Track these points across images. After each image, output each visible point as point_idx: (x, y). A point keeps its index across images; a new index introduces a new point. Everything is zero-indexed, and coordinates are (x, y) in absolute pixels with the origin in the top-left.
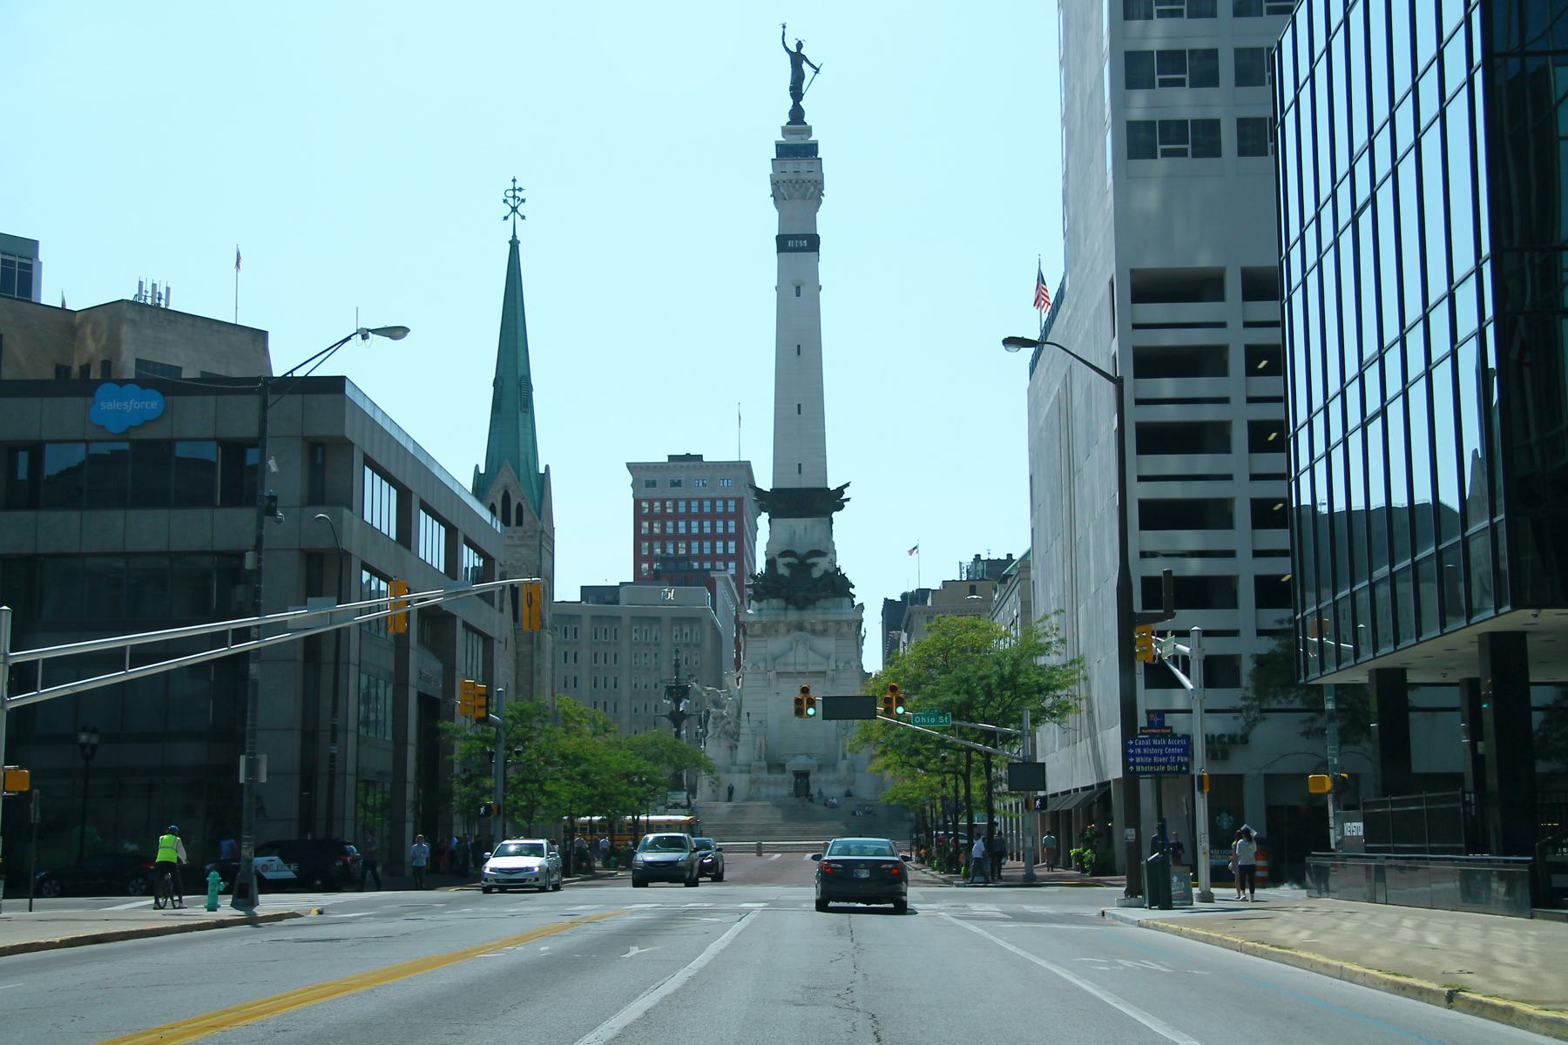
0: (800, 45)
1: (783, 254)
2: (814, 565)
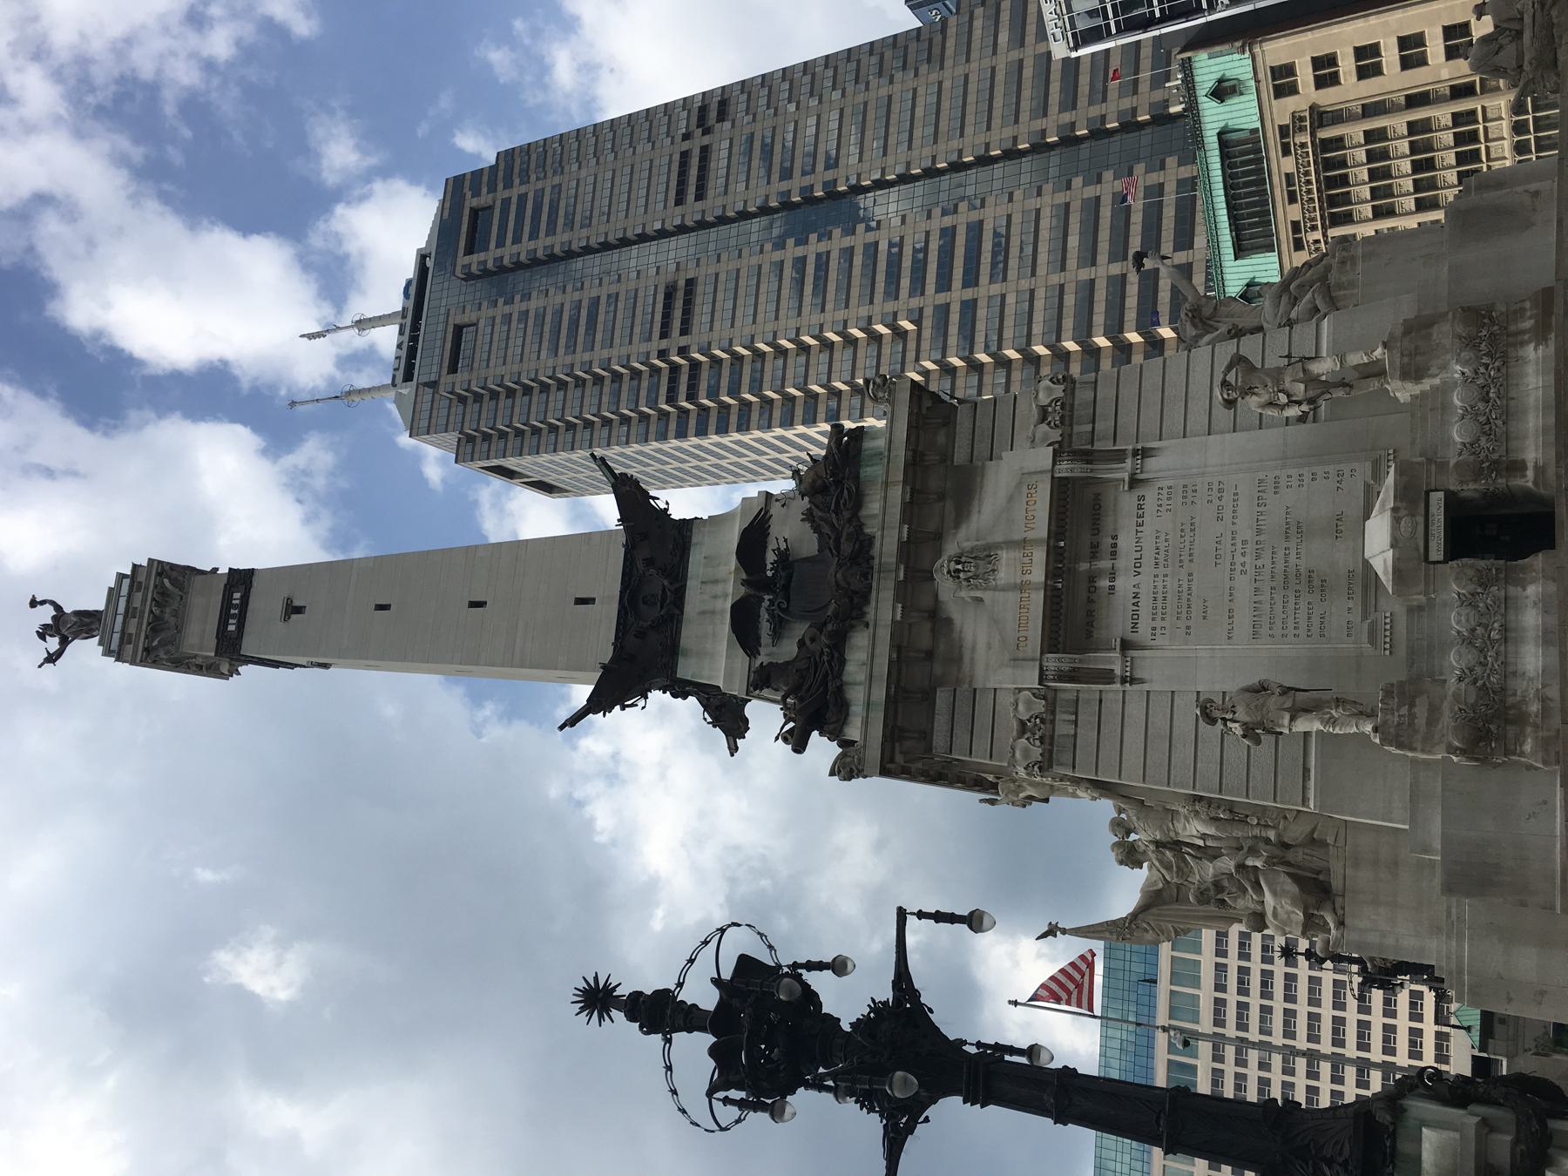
2: (783, 556)
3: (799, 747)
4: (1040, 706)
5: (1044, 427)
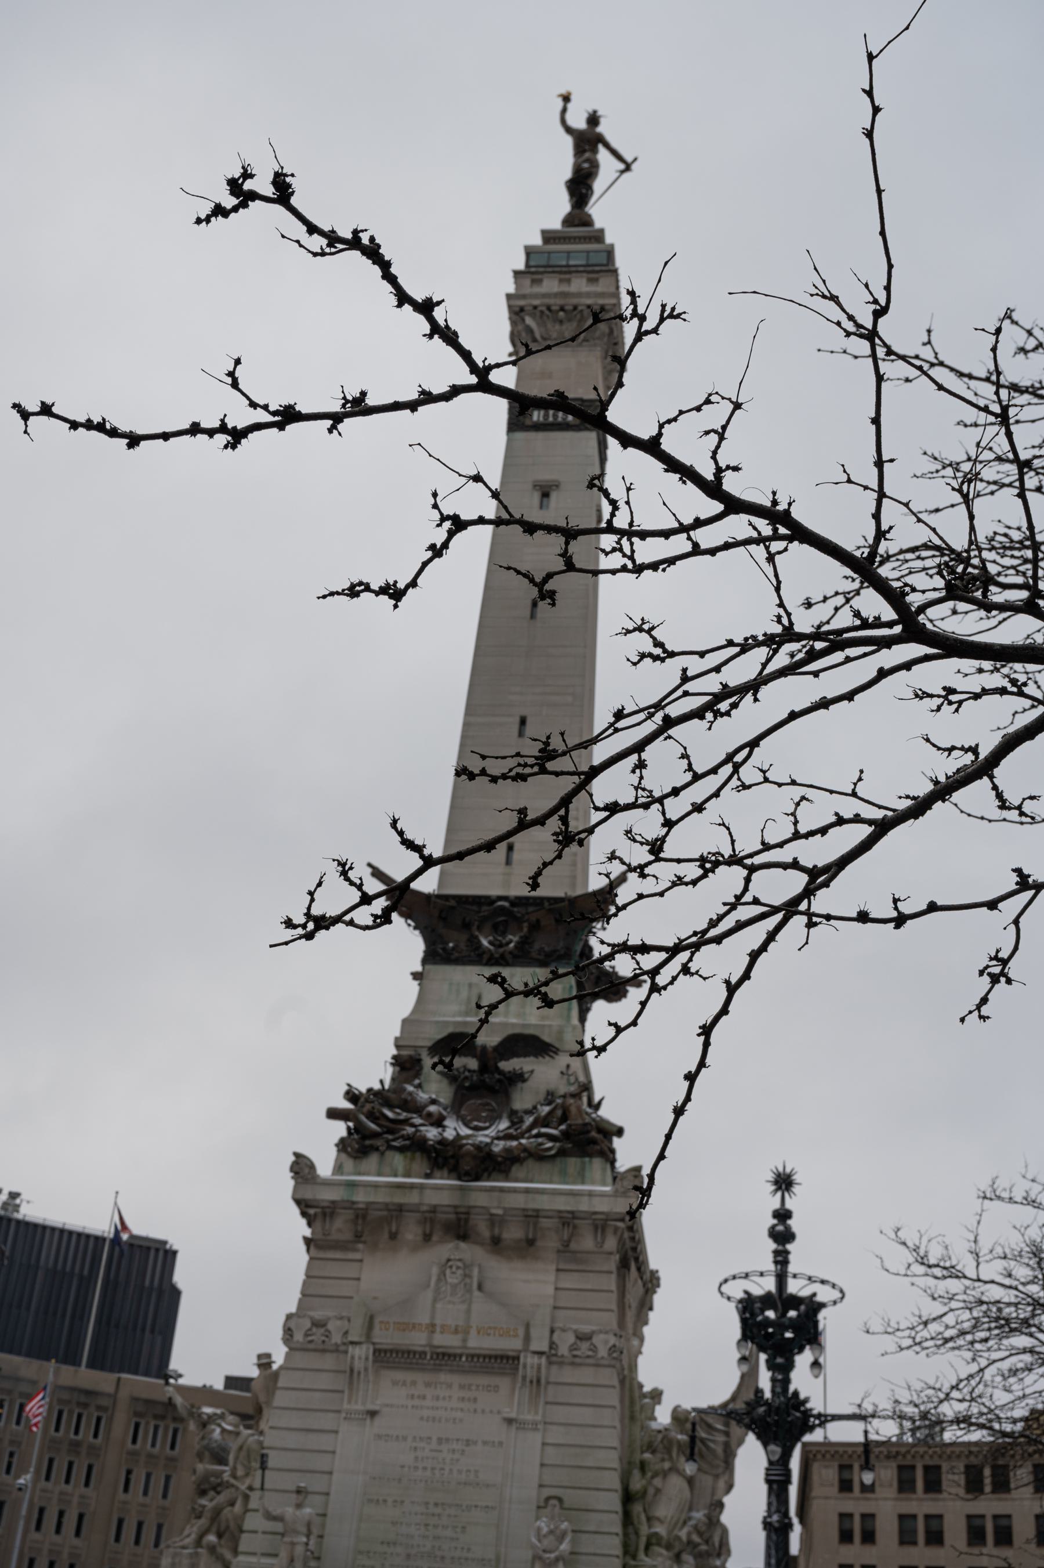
0: (593, 120)
1: (520, 435)
2: (519, 1077)
3: (333, 1114)
4: (337, 1338)
5: (571, 1338)
